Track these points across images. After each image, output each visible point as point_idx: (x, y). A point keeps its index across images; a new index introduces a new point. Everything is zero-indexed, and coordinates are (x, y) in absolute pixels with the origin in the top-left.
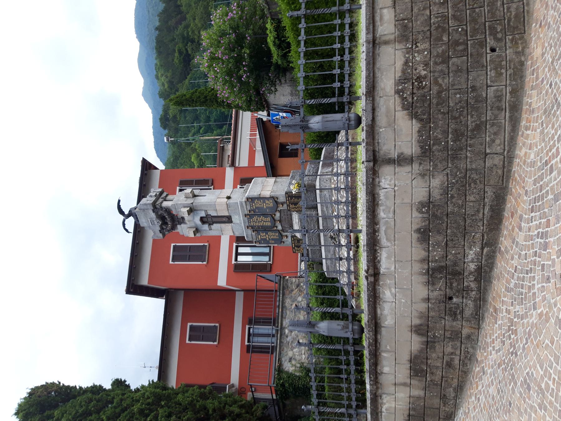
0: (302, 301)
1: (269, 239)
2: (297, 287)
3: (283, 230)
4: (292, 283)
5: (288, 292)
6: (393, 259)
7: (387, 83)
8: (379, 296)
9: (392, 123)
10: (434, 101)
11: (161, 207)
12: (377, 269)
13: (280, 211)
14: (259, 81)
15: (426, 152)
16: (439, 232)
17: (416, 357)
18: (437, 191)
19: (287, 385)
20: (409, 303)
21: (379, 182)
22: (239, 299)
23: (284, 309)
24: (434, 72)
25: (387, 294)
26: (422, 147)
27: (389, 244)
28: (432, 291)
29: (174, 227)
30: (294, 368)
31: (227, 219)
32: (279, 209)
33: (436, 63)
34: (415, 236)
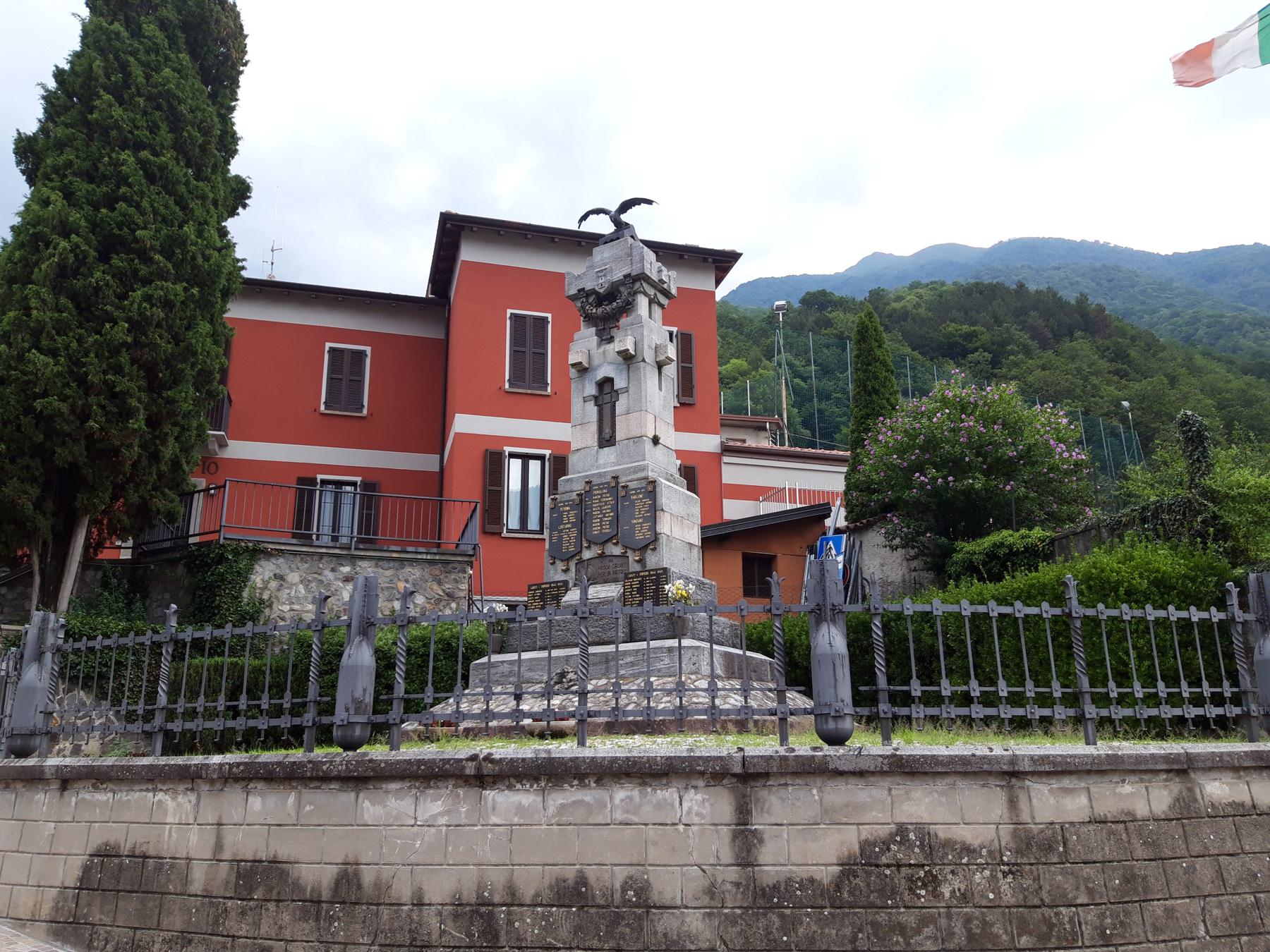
3: (581, 561)
4: (456, 581)
5: (437, 572)
6: (516, 820)
7: (921, 805)
8: (429, 787)
10: (882, 917)
11: (635, 293)
12: (494, 783)
13: (624, 556)
14: (914, 510)
15: (766, 898)
16: (577, 929)
17: (283, 875)
18: (676, 924)
19: (221, 569)
20: (413, 859)
21: (695, 787)
22: (425, 462)
23: (397, 564)
25: (435, 805)
26: (775, 887)
28: (440, 914)
29: (590, 319)
30: (259, 585)
31: (607, 437)
32: (630, 553)
33: (968, 920)
34: (570, 873)
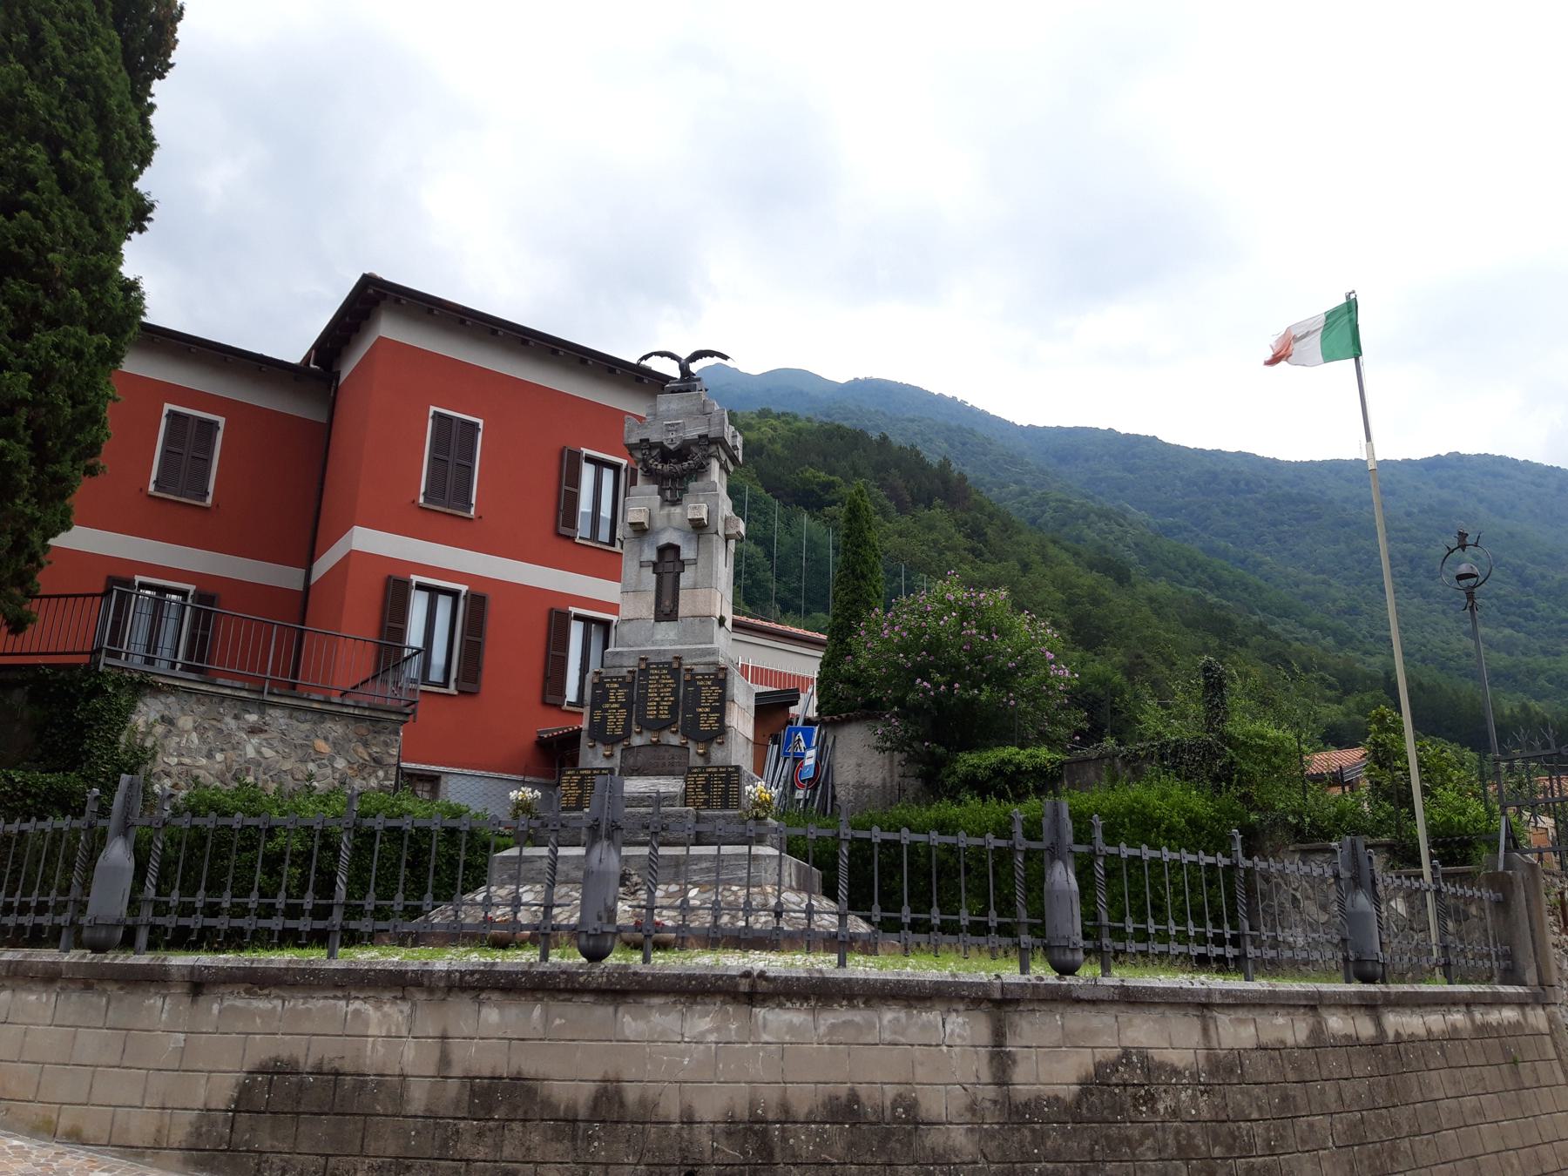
0: (334, 769)
1: (606, 710)
2: (374, 760)
3: (629, 748)
4: (386, 744)
5: (364, 732)
6: (787, 1038)
7: (1142, 1032)
8: (695, 1002)
9: (1070, 1041)
10: (1113, 1131)
11: (710, 456)
12: (764, 1000)
13: (684, 747)
14: (908, 712)
15: (1019, 1113)
16: (851, 1145)
17: (531, 1093)
18: (942, 1140)
19: (97, 703)
20: (681, 1076)
21: (956, 1011)
22: (288, 577)
23: (316, 717)
24: (1164, 1130)
25: (703, 1022)
26: (1026, 1105)
27: (822, 1029)
28: (712, 1132)
29: (651, 475)
30: (141, 729)
31: (667, 610)
32: (691, 745)
33: (1178, 1132)
34: (843, 1091)
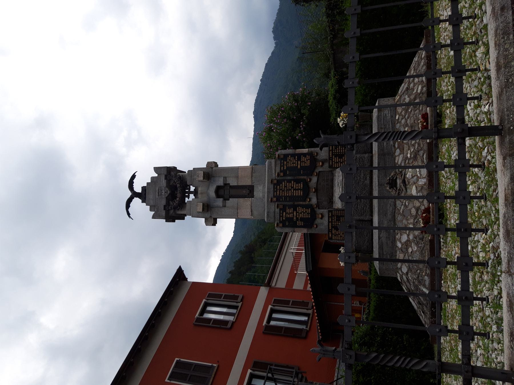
1: (297, 219)
3: (318, 206)
13: (318, 175)
